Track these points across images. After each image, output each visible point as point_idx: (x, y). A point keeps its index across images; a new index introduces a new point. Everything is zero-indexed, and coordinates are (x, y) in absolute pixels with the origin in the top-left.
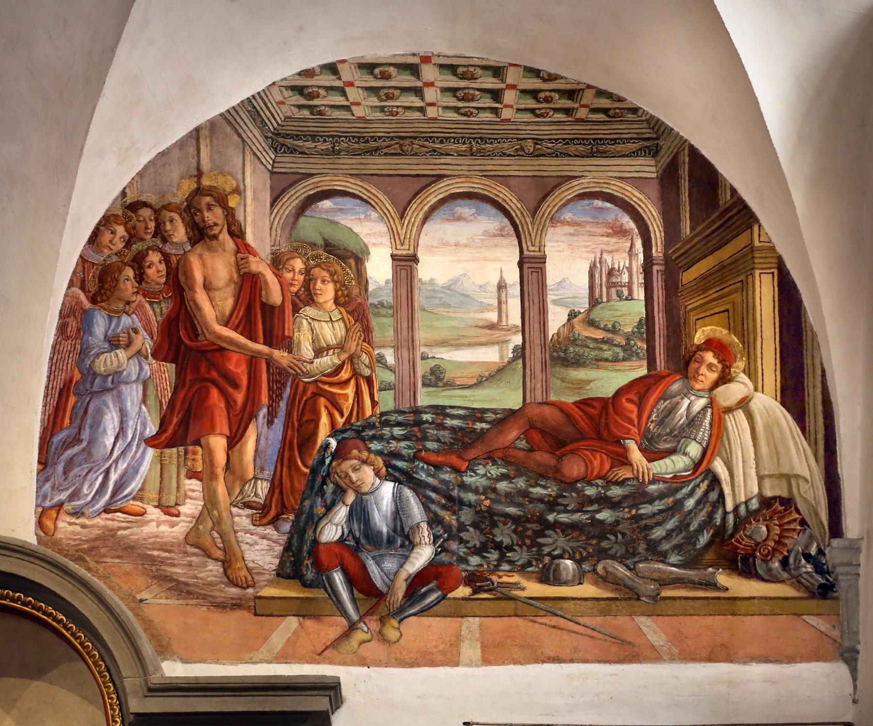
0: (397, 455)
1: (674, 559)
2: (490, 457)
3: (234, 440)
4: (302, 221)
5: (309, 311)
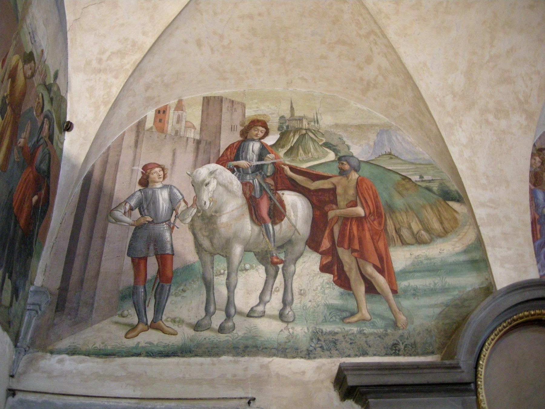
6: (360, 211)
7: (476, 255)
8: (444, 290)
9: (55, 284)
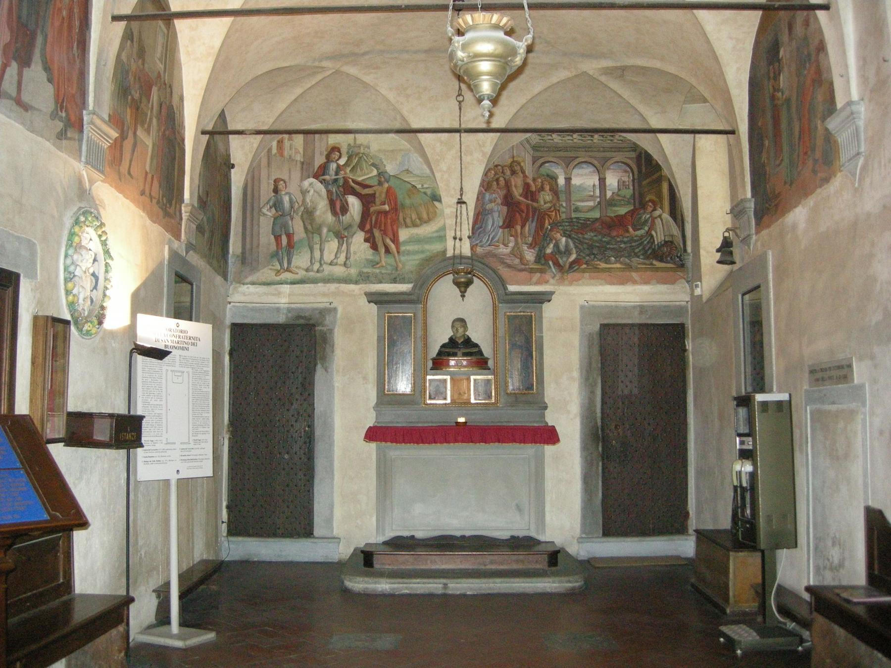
2: (591, 230)
3: (523, 226)
6: (387, 207)
7: (442, 234)
8: (423, 252)
9: (239, 251)
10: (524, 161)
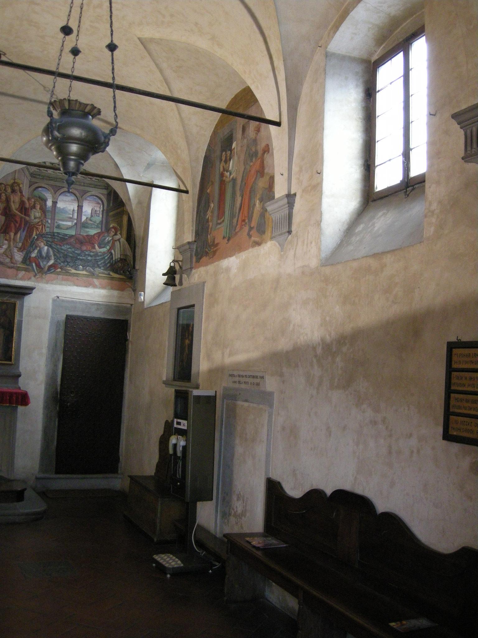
0: (48, 241)
1: (102, 268)
2: (67, 244)
3: (16, 234)
4: (35, 192)
5: (34, 210)
10: (23, 184)
